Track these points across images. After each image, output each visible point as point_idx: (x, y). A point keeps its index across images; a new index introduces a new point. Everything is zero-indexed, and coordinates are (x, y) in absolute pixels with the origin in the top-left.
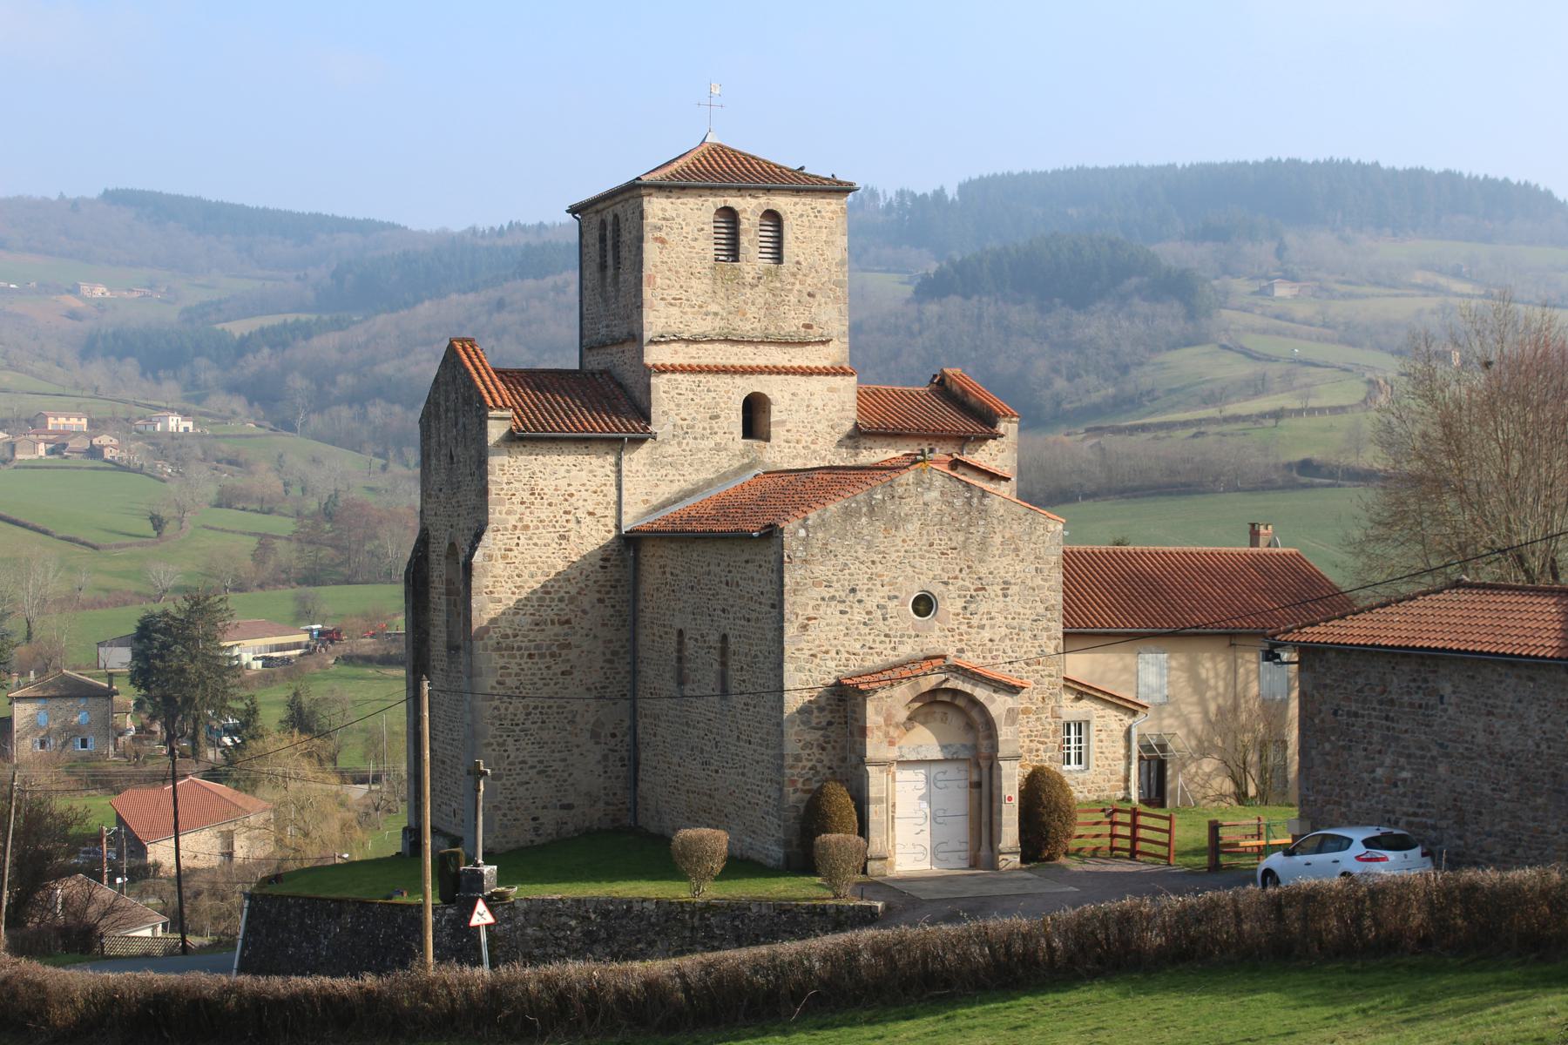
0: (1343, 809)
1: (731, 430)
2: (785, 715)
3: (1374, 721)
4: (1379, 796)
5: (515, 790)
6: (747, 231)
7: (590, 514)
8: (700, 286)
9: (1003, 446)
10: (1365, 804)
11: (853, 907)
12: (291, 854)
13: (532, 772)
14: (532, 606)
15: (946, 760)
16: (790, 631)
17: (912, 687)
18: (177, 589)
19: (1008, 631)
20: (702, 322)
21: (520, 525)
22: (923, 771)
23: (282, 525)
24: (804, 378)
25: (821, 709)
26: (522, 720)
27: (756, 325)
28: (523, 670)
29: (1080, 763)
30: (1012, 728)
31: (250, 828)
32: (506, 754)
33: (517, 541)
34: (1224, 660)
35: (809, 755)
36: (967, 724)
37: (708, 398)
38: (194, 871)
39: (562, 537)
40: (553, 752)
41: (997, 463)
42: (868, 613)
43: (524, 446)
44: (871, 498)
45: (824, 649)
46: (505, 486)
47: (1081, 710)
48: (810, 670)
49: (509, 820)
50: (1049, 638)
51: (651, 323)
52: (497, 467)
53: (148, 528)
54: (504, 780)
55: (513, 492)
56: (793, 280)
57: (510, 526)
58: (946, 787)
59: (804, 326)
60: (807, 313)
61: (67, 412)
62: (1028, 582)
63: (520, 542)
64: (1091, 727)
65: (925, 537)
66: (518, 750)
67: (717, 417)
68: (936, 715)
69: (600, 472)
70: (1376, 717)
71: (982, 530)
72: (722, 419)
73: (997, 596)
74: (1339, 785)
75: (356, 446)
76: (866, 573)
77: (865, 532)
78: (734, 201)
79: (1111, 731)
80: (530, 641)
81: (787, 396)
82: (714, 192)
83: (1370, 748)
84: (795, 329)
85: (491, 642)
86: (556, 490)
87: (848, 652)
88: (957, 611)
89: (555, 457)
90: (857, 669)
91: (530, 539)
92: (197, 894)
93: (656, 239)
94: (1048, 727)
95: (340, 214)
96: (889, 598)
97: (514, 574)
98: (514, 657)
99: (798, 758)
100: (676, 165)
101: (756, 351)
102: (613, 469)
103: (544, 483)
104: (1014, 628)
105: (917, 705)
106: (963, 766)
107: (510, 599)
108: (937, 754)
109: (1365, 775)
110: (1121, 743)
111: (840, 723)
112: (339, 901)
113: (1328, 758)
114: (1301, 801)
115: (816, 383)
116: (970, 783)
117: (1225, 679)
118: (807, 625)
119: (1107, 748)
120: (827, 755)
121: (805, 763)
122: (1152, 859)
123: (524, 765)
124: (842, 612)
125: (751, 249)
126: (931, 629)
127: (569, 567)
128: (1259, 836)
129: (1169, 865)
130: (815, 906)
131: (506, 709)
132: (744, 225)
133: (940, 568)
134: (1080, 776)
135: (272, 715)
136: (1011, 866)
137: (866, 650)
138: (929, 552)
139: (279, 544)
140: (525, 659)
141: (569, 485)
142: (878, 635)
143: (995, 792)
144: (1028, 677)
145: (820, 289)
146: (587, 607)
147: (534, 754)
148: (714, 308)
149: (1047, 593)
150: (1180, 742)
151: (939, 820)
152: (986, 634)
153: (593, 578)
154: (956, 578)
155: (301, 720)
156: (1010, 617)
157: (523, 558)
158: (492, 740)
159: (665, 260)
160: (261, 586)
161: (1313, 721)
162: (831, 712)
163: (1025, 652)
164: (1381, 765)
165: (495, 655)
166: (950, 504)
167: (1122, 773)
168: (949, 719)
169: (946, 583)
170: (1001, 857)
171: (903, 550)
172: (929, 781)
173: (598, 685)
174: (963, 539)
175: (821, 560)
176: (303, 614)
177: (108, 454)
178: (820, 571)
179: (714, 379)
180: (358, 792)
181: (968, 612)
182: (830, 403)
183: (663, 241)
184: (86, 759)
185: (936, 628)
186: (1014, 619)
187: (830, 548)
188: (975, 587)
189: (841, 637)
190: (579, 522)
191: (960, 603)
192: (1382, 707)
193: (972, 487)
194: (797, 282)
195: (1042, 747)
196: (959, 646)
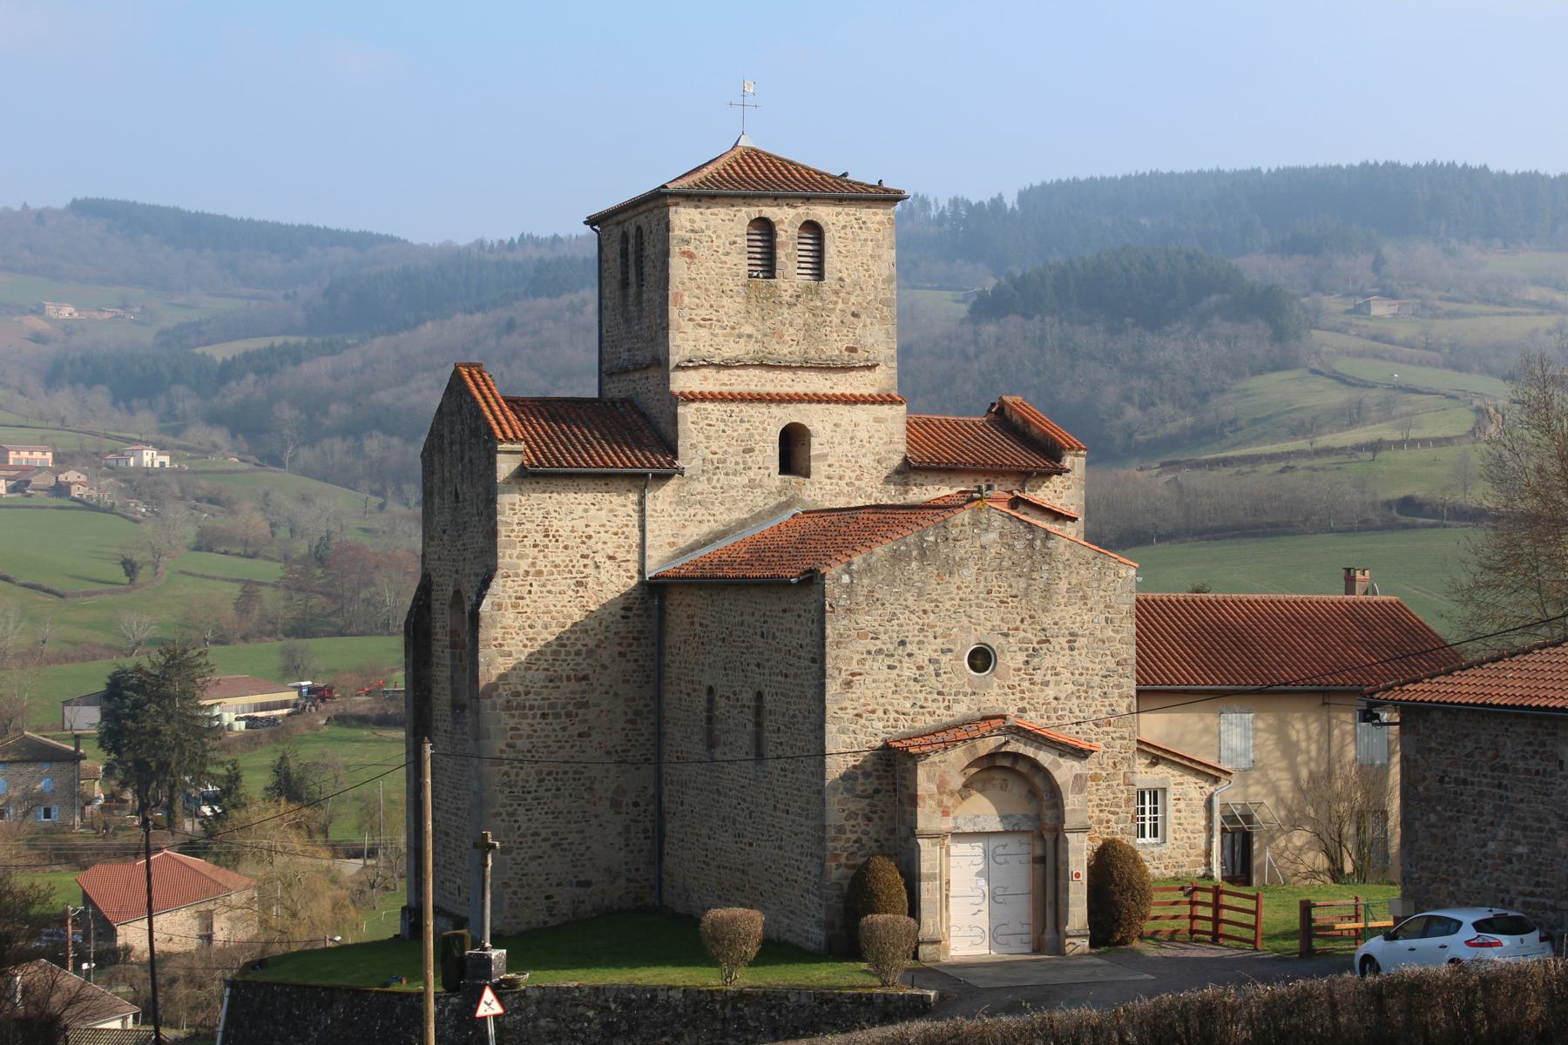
0: (1451, 888)
1: (767, 465)
2: (827, 782)
3: (1485, 789)
4: (1491, 874)
5: (526, 865)
6: (784, 244)
7: (611, 558)
8: (732, 306)
9: (1069, 483)
10: (1476, 883)
11: (903, 996)
12: (277, 936)
13: (546, 846)
14: (546, 661)
15: (1005, 832)
16: (833, 688)
17: (968, 750)
18: (152, 642)
19: (1075, 688)
20: (734, 344)
21: (532, 570)
22: (980, 844)
23: (268, 570)
24: (848, 407)
25: (867, 775)
26: (534, 788)
27: (794, 348)
28: (535, 731)
29: (1156, 835)
30: (1080, 797)
31: (231, 908)
32: (516, 825)
33: (529, 588)
34: (1317, 721)
35: (853, 826)
36: (1030, 791)
37: (742, 429)
38: (169, 956)
39: (579, 584)
40: (569, 822)
41: (1062, 501)
42: (920, 668)
43: (538, 483)
44: (922, 540)
45: (870, 708)
46: (516, 528)
47: (1156, 777)
48: (854, 732)
49: (519, 899)
50: (1121, 696)
51: (678, 346)
52: (507, 507)
53: (119, 574)
54: (514, 854)
55: (524, 534)
56: (835, 299)
57: (521, 572)
59: (847, 349)
60: (851, 335)
61: (31, 445)
62: (1098, 633)
63: (532, 589)
64: (1168, 796)
65: (983, 584)
66: (529, 820)
67: (751, 450)
68: (995, 782)
69: (621, 511)
70: (1488, 785)
71: (1045, 575)
72: (757, 452)
73: (1062, 648)
74: (1447, 862)
75: (350, 484)
76: (917, 623)
77: (916, 577)
78: (770, 212)
79: (1191, 800)
80: (543, 699)
81: (829, 427)
82: (748, 201)
83: (1481, 819)
84: (837, 352)
85: (500, 701)
86: (573, 531)
87: (897, 712)
88: (1017, 666)
89: (572, 495)
90: (906, 730)
91: (544, 585)
92: (173, 981)
93: (683, 253)
94: (1120, 795)
95: (333, 226)
96: (943, 652)
97: (526, 624)
98: (525, 717)
99: (841, 830)
100: (705, 171)
101: (794, 377)
102: (636, 508)
103: (560, 523)
105: (974, 770)
106: (1025, 839)
107: (521, 652)
108: (996, 825)
109: (1475, 850)
110: (1202, 813)
111: (888, 791)
112: (331, 990)
113: (1434, 830)
114: (1404, 879)
115: (861, 413)
117: (1318, 741)
118: (851, 681)
119: (1185, 818)
120: (874, 826)
121: (849, 835)
122: (1238, 943)
123: (537, 838)
124: (890, 667)
125: (789, 264)
126: (989, 686)
127: (587, 617)
128: (1357, 918)
129: (1256, 949)
130: (860, 995)
131: (517, 775)
132: (781, 237)
133: (999, 618)
134: (1156, 850)
135: (256, 782)
136: (1079, 950)
137: (917, 709)
138: (986, 600)
139: (265, 592)
140: (538, 720)
141: (587, 526)
142: (931, 693)
143: (1061, 868)
145: (866, 308)
146: (607, 663)
147: (548, 824)
148: (747, 329)
149: (1119, 646)
150: (1268, 811)
151: (999, 899)
152: (1051, 692)
153: (613, 628)
154: (1017, 629)
155: (288, 787)
156: (1077, 672)
157: (535, 607)
158: (501, 810)
159: (693, 276)
160: (245, 638)
161: (1416, 789)
162: (878, 778)
164: (1493, 839)
165: (504, 715)
166: (1011, 547)
167: (1203, 848)
168: (1010, 786)
169: (1006, 635)
170: (1067, 941)
171: (958, 598)
173: (619, 749)
174: (1025, 585)
175: (867, 608)
176: (291, 670)
177: (76, 492)
178: (866, 621)
179: (749, 409)
180: (352, 867)
181: (1031, 667)
182: (876, 435)
183: (691, 256)
184: (49, 831)
185: (995, 685)
186: (1081, 674)
187: (876, 595)
188: (1038, 639)
189: (890, 695)
190: (598, 567)
191: (1022, 657)
192: (1495, 774)
193: (1035, 527)
194: (840, 301)
195: (1113, 818)
196: (1021, 704)
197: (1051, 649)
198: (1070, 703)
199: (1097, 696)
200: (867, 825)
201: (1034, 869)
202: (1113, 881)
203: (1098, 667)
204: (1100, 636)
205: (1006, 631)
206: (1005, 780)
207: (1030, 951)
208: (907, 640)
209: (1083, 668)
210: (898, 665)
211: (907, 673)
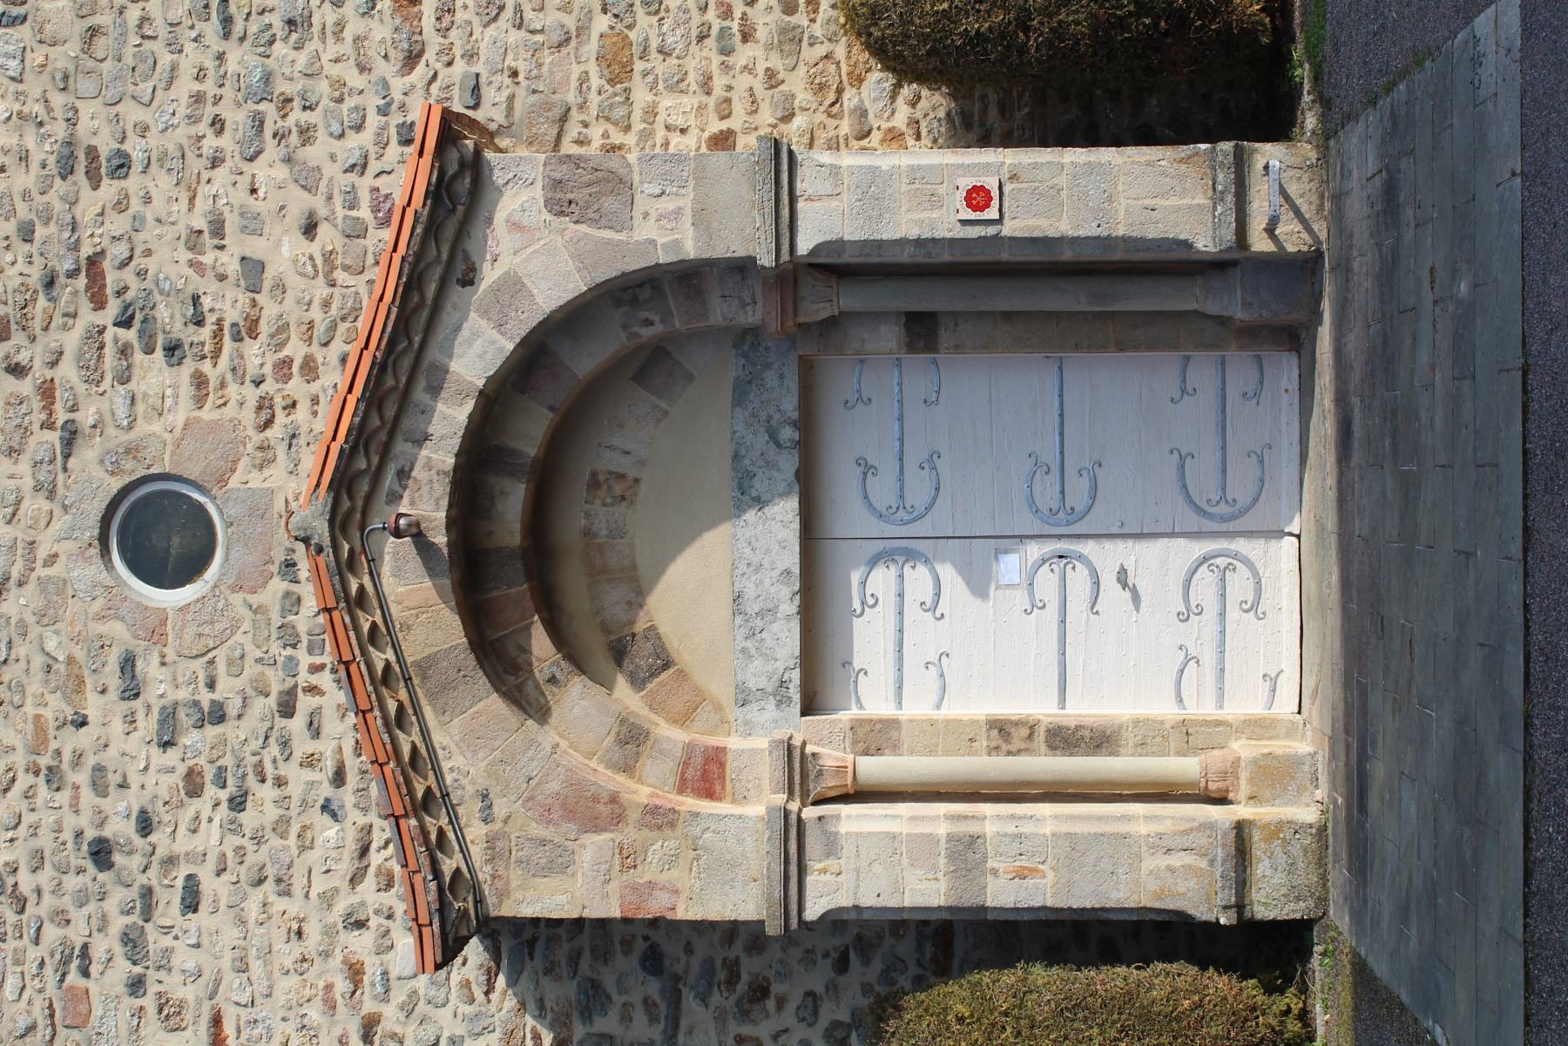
22: (855, 577)
25: (593, 999)
36: (641, 377)
42: (193, 784)
45: (342, 986)
58: (931, 461)
62: (61, 58)
73: (121, 205)
76: (28, 795)
88: (186, 389)
96: (132, 692)
104: (259, 122)
116: (911, 348)
120: (784, 975)
124: (191, 903)
126: (258, 506)
136: (1302, 190)
137: (347, 796)
142: (285, 743)
144: (471, 56)
151: (1078, 494)
154: (47, 391)
156: (210, 143)
163: (363, 68)
169: (71, 437)
170: (1260, 243)
172: (900, 553)
181: (189, 335)
185: (256, 481)
186: (218, 125)
188: (85, 306)
189: (294, 907)
191: (153, 373)
197: (121, 251)
198: (330, 170)
199: (302, 58)
200: (781, 1003)
201: (957, 348)
202: (1002, 34)
203: (192, 57)
204: (73, 48)
205: (54, 437)
206: (594, 484)
207: (1286, 370)
208: (90, 834)
209: (193, 119)
210: (183, 871)
211: (211, 837)
